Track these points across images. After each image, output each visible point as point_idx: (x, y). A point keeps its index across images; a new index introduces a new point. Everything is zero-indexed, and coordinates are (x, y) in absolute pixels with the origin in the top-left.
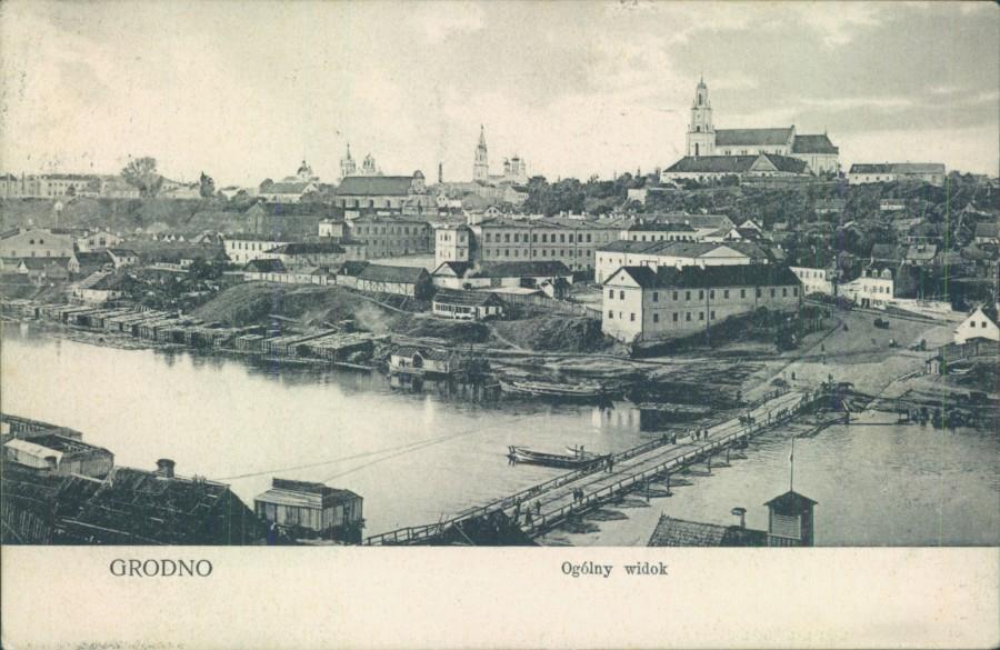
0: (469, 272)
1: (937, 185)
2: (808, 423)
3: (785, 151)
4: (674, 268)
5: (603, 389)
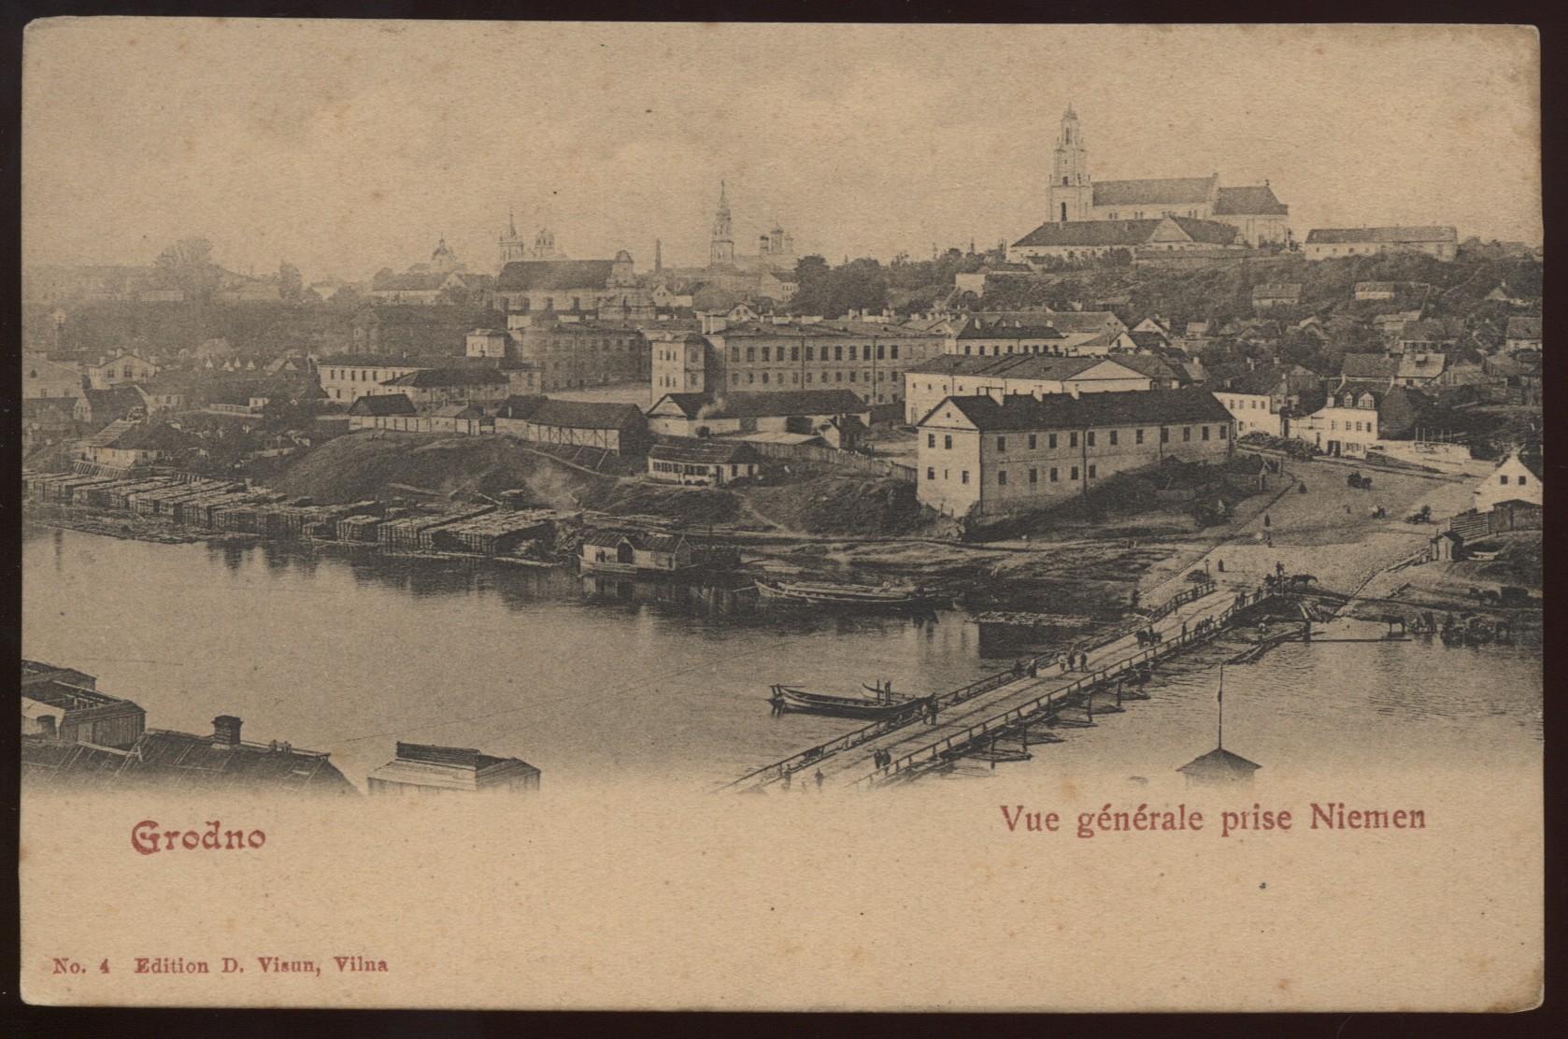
0: (705, 409)
1: (1444, 259)
2: (1248, 641)
3: (1204, 211)
4: (1030, 397)
5: (920, 591)
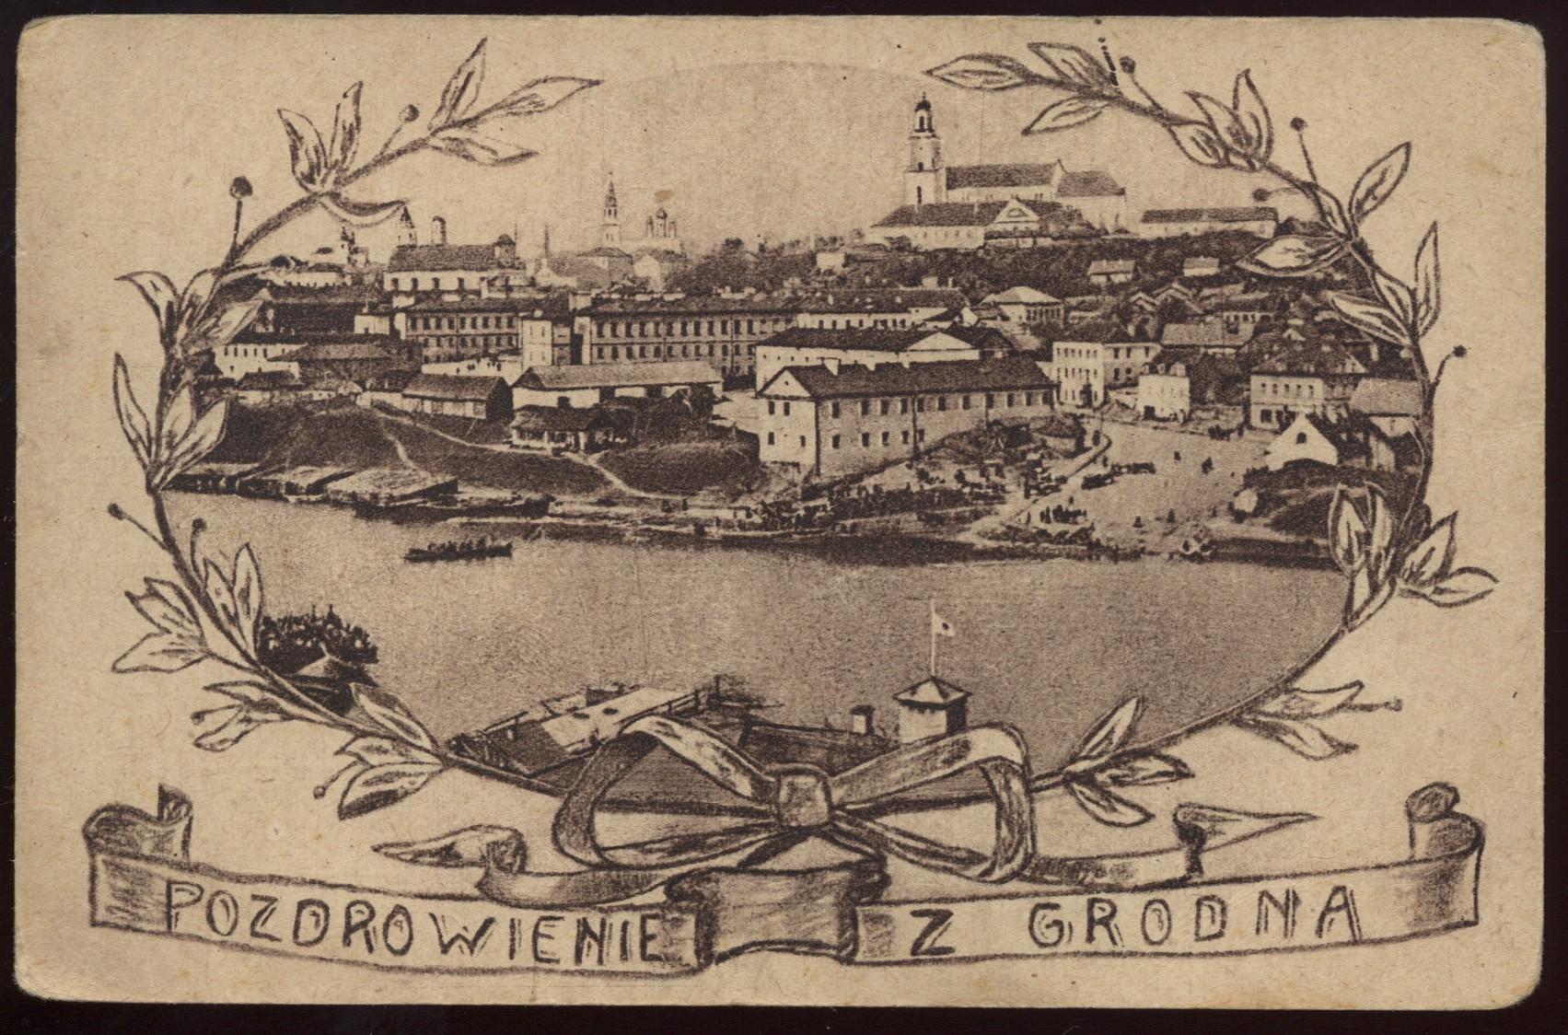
3: (1048, 193)
